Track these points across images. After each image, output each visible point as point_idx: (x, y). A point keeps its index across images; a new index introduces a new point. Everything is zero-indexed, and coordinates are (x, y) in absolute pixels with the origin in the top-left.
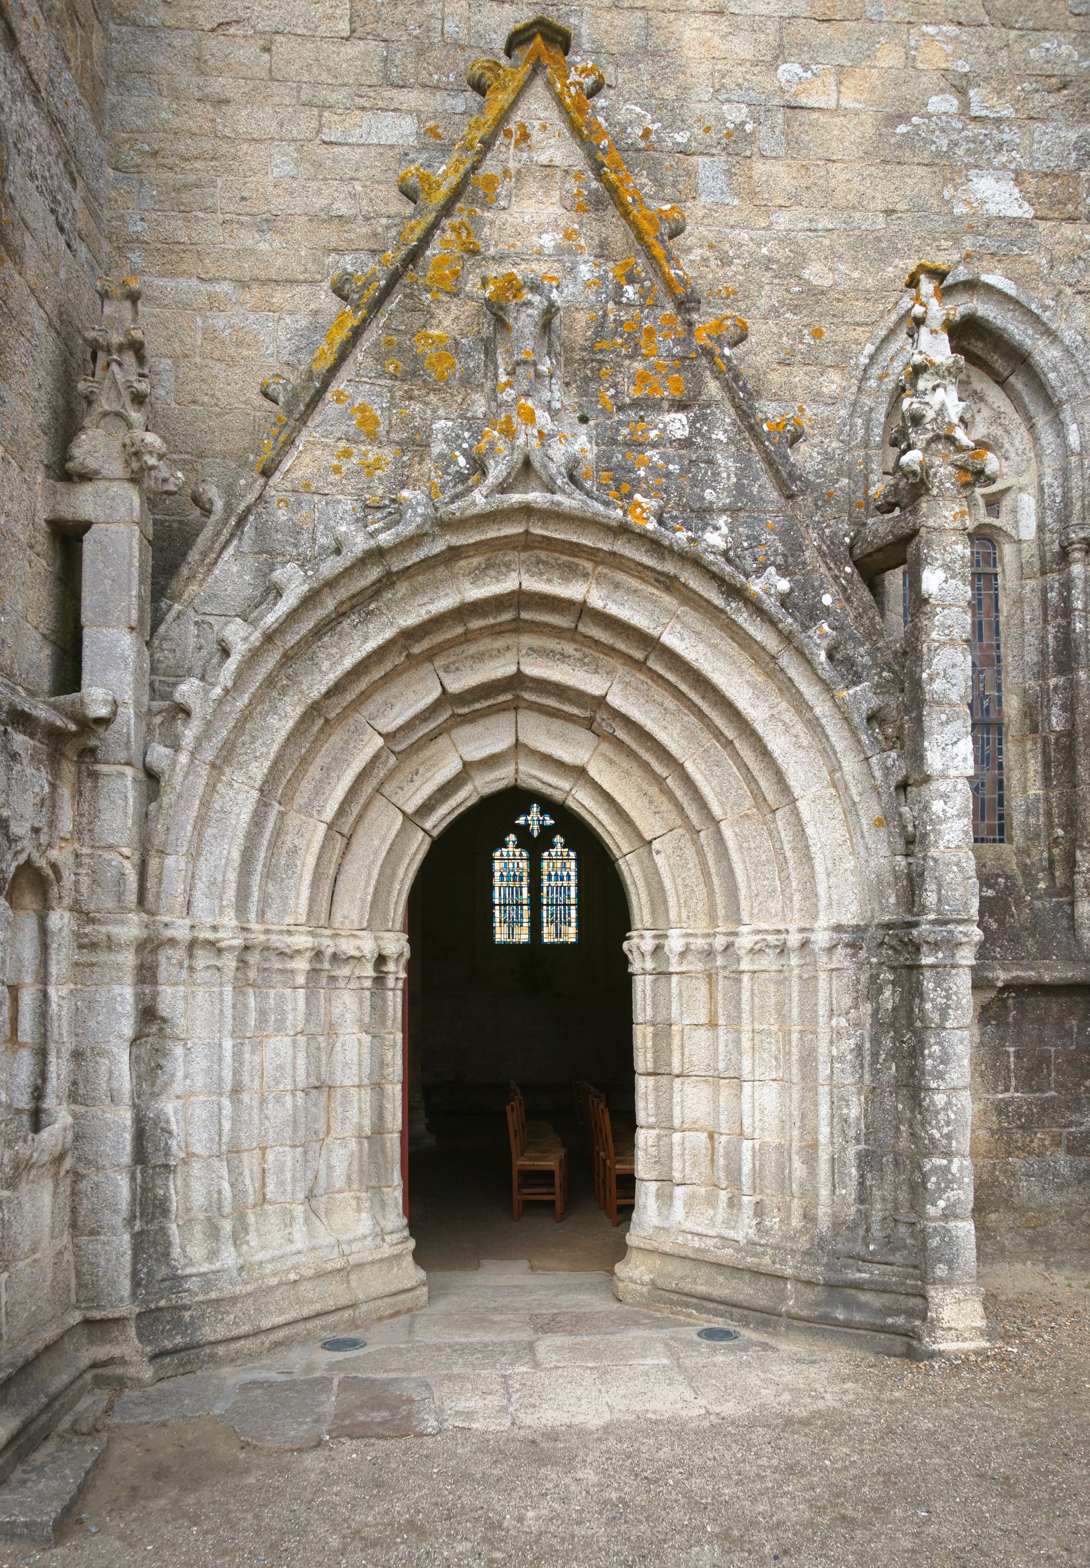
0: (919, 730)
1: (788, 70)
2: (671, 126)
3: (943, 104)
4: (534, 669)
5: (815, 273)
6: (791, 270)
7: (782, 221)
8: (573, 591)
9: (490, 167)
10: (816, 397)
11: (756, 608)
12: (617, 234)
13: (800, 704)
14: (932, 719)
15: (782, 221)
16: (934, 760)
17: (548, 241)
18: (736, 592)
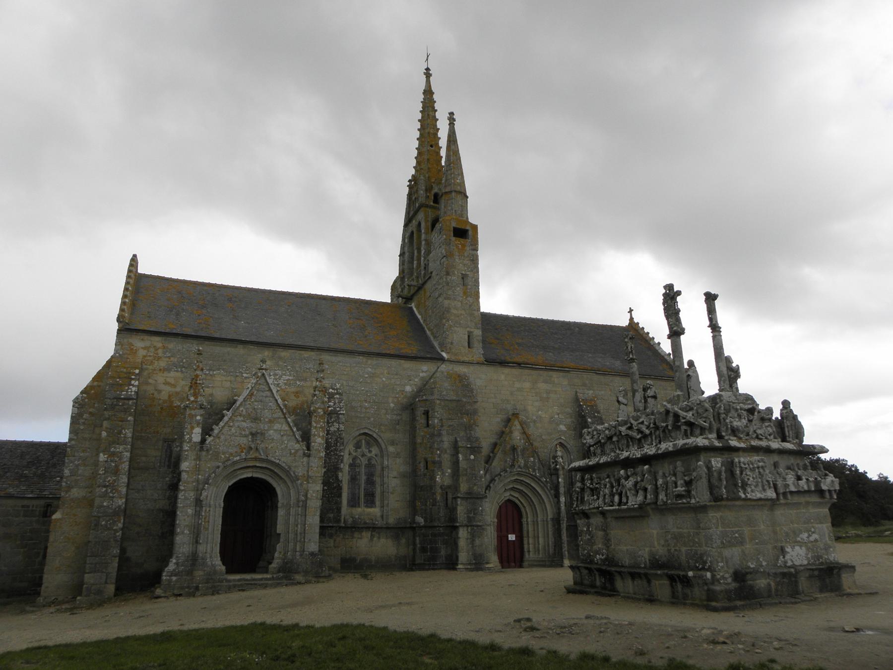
0: (559, 497)
1: (540, 412)
2: (528, 419)
3: (556, 416)
4: (515, 486)
5: (543, 437)
6: (541, 436)
7: (540, 431)
8: (521, 479)
9: (512, 429)
10: (544, 452)
11: (542, 482)
12: (525, 436)
13: (546, 492)
14: (561, 495)
15: (540, 431)
16: (561, 500)
17: (518, 438)
18: (539, 480)
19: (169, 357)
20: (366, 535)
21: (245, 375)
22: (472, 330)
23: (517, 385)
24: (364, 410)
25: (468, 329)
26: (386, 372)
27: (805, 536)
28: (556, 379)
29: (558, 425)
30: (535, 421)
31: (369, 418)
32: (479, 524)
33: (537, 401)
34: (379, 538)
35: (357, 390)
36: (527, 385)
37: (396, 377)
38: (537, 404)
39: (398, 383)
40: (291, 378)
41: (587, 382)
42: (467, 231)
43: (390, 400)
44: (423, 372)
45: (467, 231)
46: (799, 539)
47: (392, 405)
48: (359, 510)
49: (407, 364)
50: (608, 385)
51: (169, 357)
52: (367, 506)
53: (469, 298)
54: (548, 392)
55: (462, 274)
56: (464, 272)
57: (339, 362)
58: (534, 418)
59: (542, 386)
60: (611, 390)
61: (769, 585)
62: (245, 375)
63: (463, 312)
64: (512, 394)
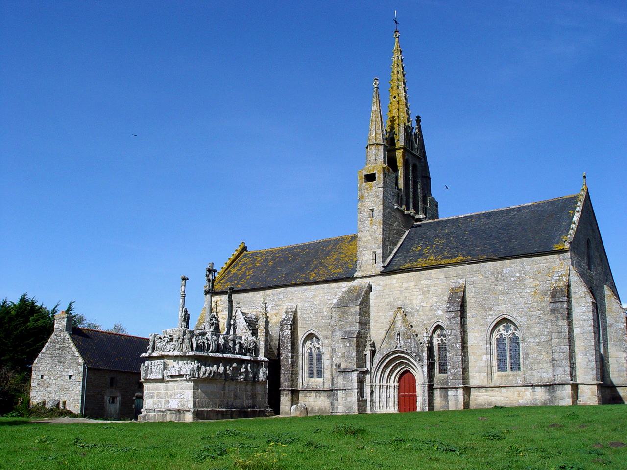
1: (422, 304)
3: (436, 304)
19: (223, 304)
20: (314, 394)
21: (253, 308)
22: (375, 250)
23: (405, 285)
24: (310, 319)
25: (373, 250)
26: (321, 292)
27: (179, 395)
28: (434, 275)
29: (436, 311)
30: (418, 311)
31: (313, 324)
32: (349, 388)
33: (420, 295)
34: (320, 396)
35: (306, 307)
36: (413, 284)
37: (327, 294)
38: (420, 297)
39: (329, 298)
40: (273, 306)
41: (461, 272)
42: (375, 174)
43: (325, 310)
44: (343, 288)
45: (375, 174)
46: (176, 397)
47: (325, 313)
48: (313, 380)
49: (333, 285)
50: (479, 271)
51: (223, 304)
52: (318, 377)
53: (374, 227)
54: (428, 287)
55: (371, 209)
56: (371, 208)
57: (296, 291)
58: (418, 308)
59: (424, 282)
60: (482, 275)
61: (155, 415)
62: (253, 308)
63: (370, 238)
64: (401, 292)
